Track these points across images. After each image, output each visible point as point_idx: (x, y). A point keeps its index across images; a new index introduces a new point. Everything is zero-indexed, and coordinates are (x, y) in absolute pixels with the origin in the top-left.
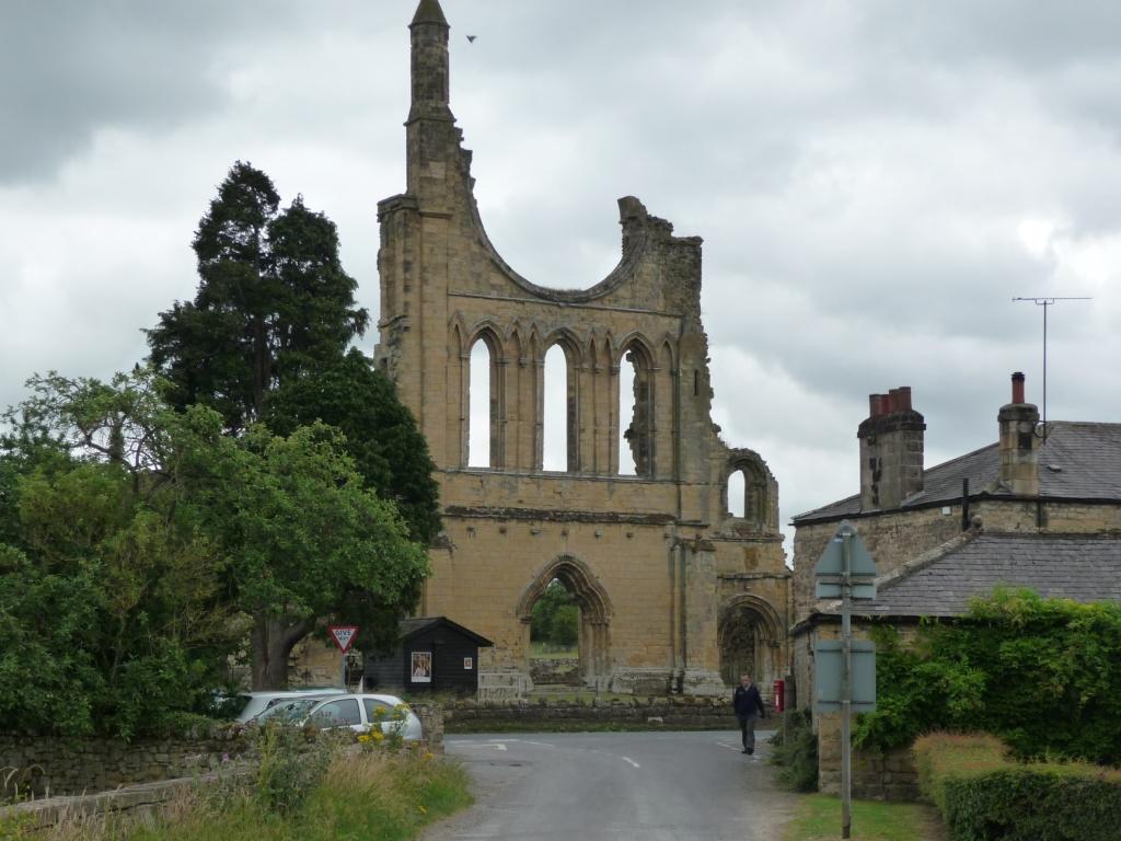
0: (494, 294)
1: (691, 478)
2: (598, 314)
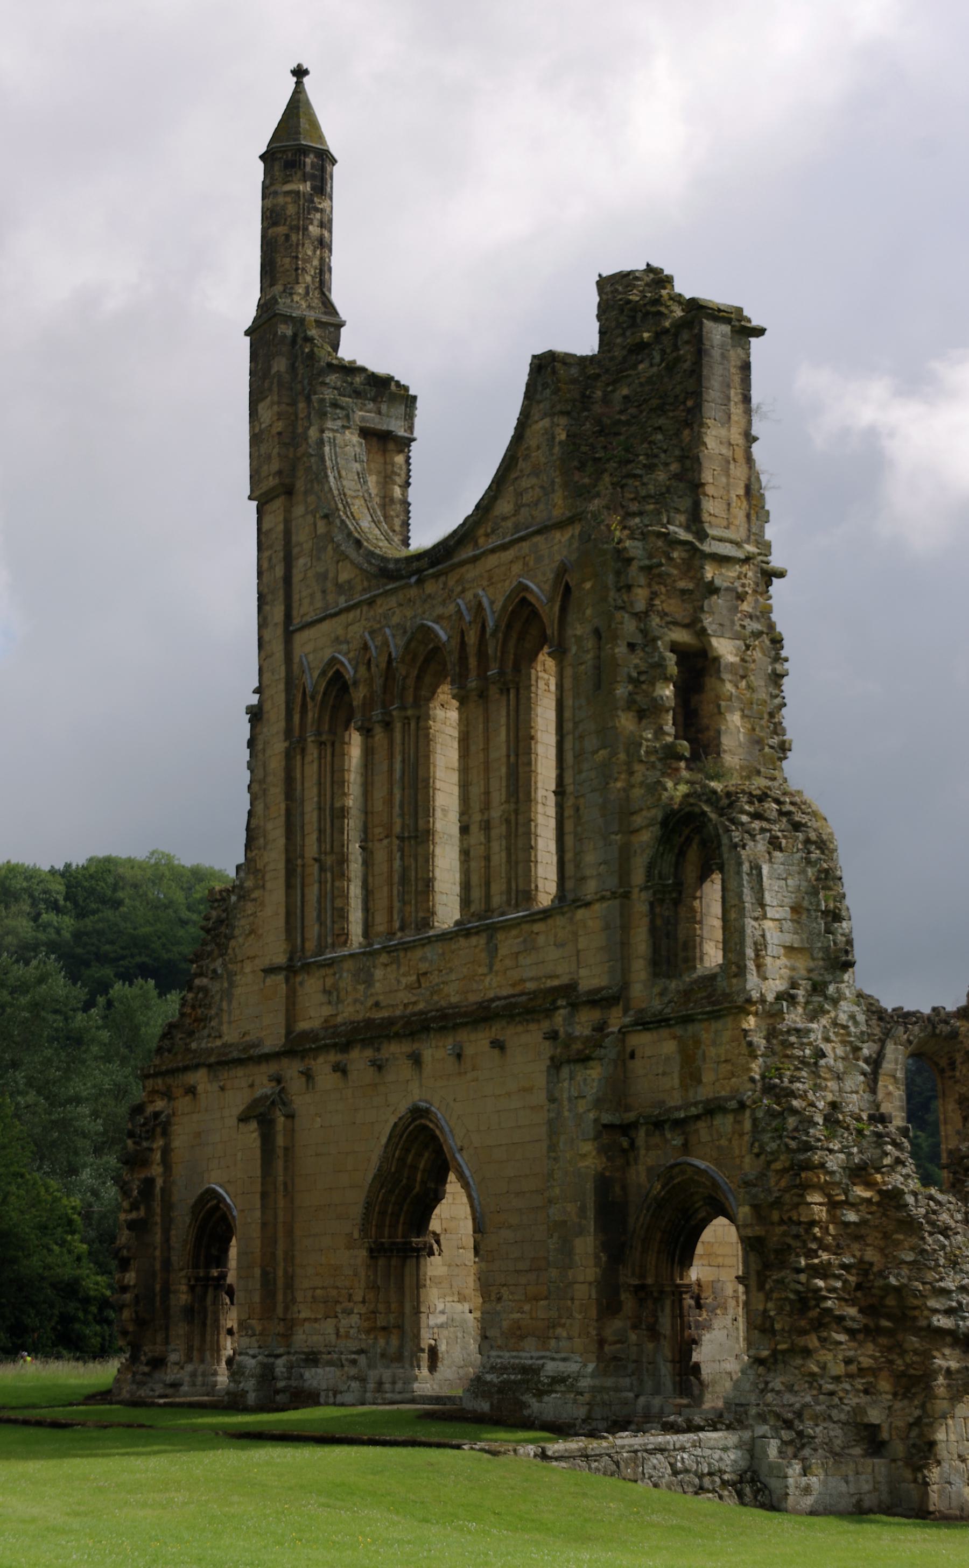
0: (342, 602)
1: (591, 888)
2: (470, 572)
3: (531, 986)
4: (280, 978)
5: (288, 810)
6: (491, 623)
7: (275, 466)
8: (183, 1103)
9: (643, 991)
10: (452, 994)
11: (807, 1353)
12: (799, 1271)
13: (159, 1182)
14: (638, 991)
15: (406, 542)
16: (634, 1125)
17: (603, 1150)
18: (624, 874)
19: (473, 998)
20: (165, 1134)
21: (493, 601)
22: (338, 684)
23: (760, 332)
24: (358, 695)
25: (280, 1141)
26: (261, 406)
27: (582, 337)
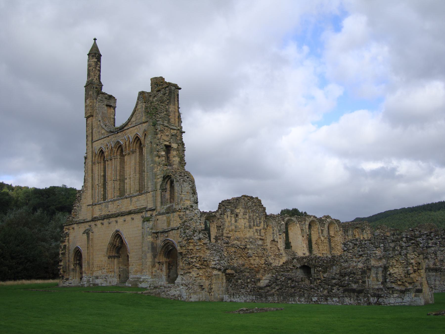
1: (150, 189)
2: (127, 131)
3: (139, 207)
4: (91, 206)
5: (92, 176)
6: (131, 141)
7: (90, 111)
8: (71, 231)
9: (159, 208)
10: (124, 209)
11: (190, 273)
12: (189, 258)
13: (67, 246)
14: (158, 208)
15: (114, 126)
16: (158, 232)
17: (152, 237)
18: (156, 187)
19: (128, 210)
20: (68, 236)
21: (132, 137)
22: (102, 152)
23: (180, 89)
24: (106, 154)
25: (91, 237)
26: (87, 100)
27: (148, 89)
